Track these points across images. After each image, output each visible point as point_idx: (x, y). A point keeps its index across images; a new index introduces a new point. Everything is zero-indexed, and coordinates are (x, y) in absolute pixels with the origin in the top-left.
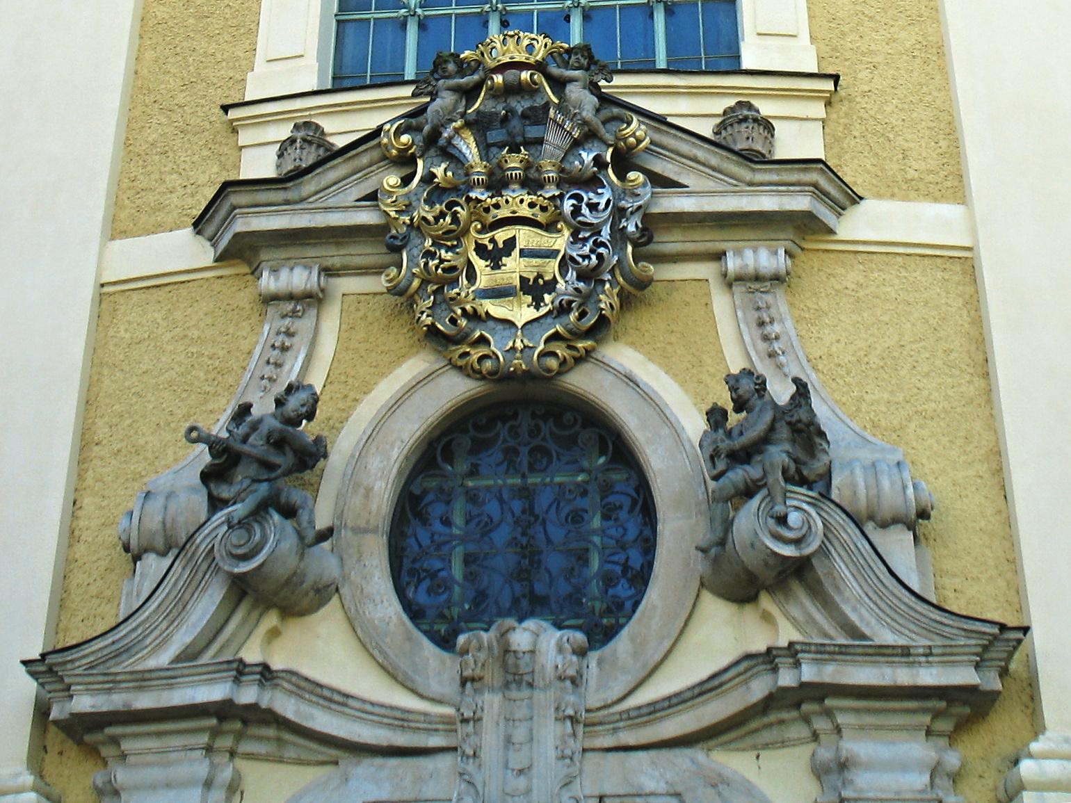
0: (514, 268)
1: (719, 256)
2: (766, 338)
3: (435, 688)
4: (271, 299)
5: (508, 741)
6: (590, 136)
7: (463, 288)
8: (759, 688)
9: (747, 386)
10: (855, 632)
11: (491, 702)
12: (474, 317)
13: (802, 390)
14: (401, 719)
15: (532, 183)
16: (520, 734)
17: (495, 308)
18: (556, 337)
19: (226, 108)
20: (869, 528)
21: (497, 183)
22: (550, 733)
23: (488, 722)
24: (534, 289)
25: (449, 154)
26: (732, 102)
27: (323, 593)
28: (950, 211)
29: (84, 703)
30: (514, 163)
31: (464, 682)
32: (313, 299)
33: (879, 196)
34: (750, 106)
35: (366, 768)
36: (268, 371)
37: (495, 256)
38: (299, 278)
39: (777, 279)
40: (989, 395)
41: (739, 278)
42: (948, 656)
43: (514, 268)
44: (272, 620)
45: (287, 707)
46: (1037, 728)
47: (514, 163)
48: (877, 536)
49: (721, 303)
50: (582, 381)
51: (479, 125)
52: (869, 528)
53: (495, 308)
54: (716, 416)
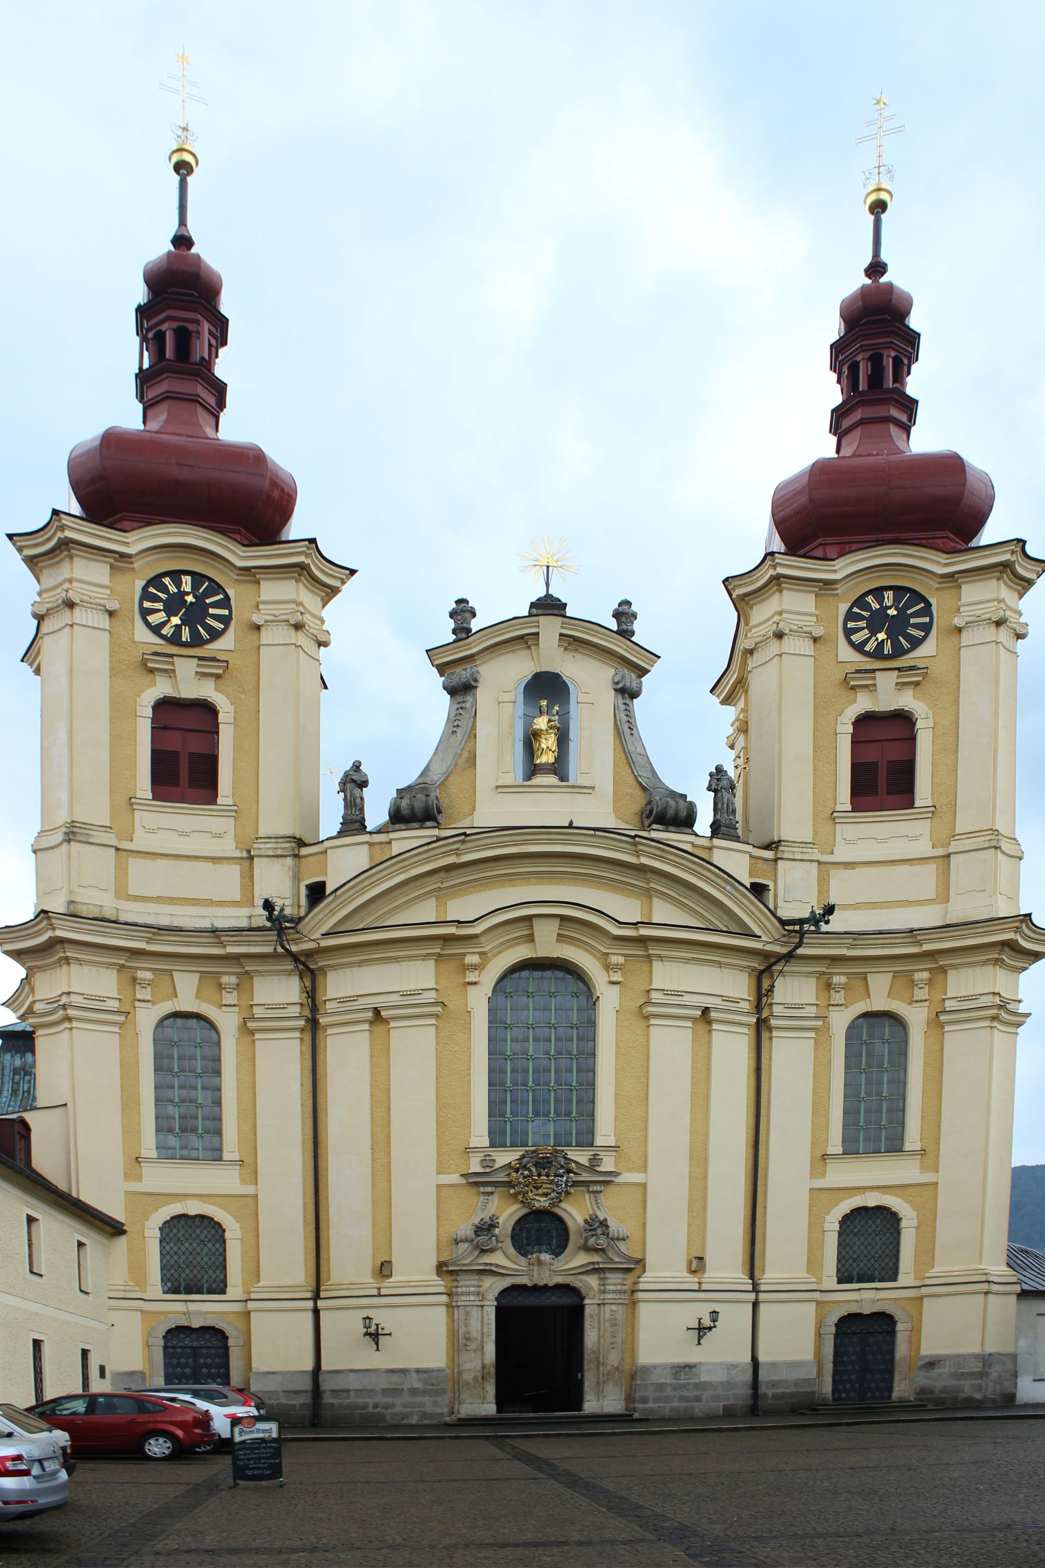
1: (588, 1186)
2: (597, 1204)
3: (523, 1264)
4: (483, 1193)
5: (539, 1274)
7: (530, 1195)
9: (594, 1217)
10: (611, 1259)
11: (536, 1268)
12: (532, 1199)
13: (605, 1220)
14: (517, 1270)
16: (542, 1273)
17: (537, 1198)
18: (550, 1203)
19: (466, 1149)
20: (615, 1241)
23: (535, 1271)
24: (546, 1195)
26: (593, 1153)
27: (498, 1249)
28: (643, 1175)
29: (451, 1268)
31: (530, 1264)
32: (492, 1193)
33: (626, 1172)
34: (598, 1155)
35: (509, 1278)
36: (484, 1207)
38: (490, 1189)
39: (600, 1192)
40: (645, 1212)
41: (592, 1192)
42: (630, 1263)
44: (488, 1253)
45: (494, 1269)
46: (644, 1271)
48: (617, 1243)
50: (556, 1210)
52: (615, 1241)
53: (537, 1198)
54: (586, 1221)
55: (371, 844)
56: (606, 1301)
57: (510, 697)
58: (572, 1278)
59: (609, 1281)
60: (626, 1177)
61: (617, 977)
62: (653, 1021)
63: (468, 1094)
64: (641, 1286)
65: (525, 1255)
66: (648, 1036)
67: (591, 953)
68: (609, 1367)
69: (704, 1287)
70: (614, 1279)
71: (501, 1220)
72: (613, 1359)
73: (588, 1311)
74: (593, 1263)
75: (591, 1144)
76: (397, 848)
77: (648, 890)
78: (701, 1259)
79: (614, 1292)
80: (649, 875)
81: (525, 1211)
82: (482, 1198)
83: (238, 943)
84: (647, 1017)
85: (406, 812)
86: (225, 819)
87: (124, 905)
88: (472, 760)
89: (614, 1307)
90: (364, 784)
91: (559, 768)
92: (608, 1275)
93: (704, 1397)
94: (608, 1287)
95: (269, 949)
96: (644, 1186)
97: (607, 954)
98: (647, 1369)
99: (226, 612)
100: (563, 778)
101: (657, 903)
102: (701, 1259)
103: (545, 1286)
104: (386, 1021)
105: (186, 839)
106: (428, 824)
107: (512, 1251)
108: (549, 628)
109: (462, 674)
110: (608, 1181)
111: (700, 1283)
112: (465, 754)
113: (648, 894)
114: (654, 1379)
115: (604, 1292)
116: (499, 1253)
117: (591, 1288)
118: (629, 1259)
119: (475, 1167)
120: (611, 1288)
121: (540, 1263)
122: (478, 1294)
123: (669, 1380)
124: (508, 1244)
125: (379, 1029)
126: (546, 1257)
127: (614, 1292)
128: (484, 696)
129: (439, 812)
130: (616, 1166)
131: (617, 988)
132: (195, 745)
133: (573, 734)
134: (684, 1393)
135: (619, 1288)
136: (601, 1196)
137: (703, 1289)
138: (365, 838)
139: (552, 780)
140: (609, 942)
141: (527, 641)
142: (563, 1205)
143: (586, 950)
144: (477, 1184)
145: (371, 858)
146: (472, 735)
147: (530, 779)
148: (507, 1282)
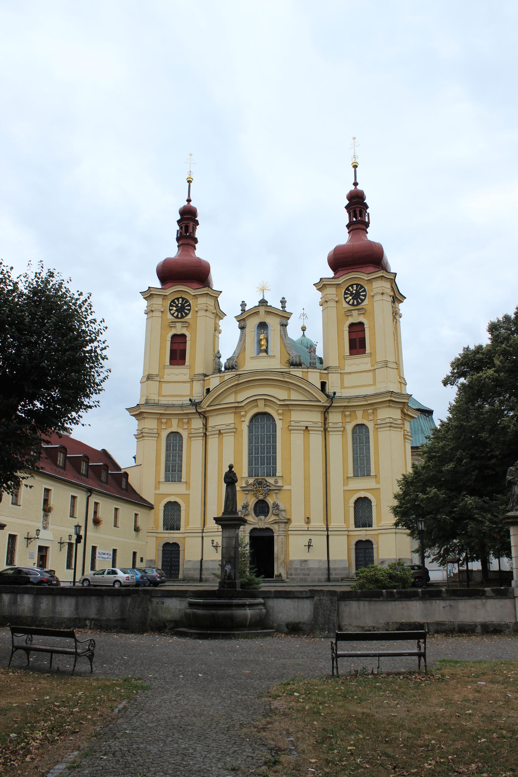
0: (260, 493)
6: (265, 484)
8: (275, 521)
14: (254, 522)
15: (261, 487)
21: (259, 487)
22: (263, 523)
25: (256, 485)
30: (260, 486)
37: (259, 492)
42: (285, 520)
43: (260, 493)
47: (260, 486)
49: (274, 495)
50: (265, 500)
51: (258, 484)
55: (220, 377)
56: (280, 534)
57: (253, 330)
58: (270, 525)
59: (281, 527)
60: (286, 487)
61: (281, 418)
62: (292, 432)
63: (242, 458)
64: (290, 529)
65: (257, 516)
66: (290, 437)
67: (274, 410)
68: (281, 561)
69: (310, 529)
70: (282, 525)
71: (250, 504)
72: (282, 557)
73: (275, 538)
74: (275, 520)
75: (276, 476)
76: (226, 378)
77: (290, 388)
78: (308, 518)
79: (282, 531)
80: (288, 383)
81: (257, 500)
82: (245, 495)
83: (187, 409)
84: (290, 430)
85: (228, 367)
86: (187, 369)
87: (161, 398)
88: (245, 349)
89: (282, 537)
90: (219, 358)
91: (266, 351)
92: (280, 524)
93: (311, 574)
94: (281, 529)
95: (195, 411)
96: (290, 490)
97: (278, 410)
98: (292, 562)
99: (189, 308)
100: (267, 354)
101: (292, 392)
102: (308, 518)
103: (263, 528)
104: (222, 434)
105: (177, 376)
106: (234, 370)
107: (254, 515)
108: (262, 310)
109: (242, 324)
110: (279, 489)
111: (308, 528)
112: (243, 348)
113: (289, 389)
114: (294, 566)
115: (279, 531)
116: (250, 516)
117: (276, 529)
118: (286, 519)
119: (244, 485)
120: (281, 529)
121: (261, 520)
122: (244, 531)
123: (299, 567)
124: (252, 512)
125: (221, 436)
126: (263, 517)
127: (282, 531)
128: (247, 329)
129: (236, 366)
130: (282, 483)
131: (281, 421)
132: (181, 347)
133: (269, 341)
134: (303, 572)
135: (283, 529)
136: (278, 494)
137: (309, 530)
138: (219, 375)
139: (264, 354)
140: (278, 406)
141: (257, 313)
142: (268, 498)
143: (273, 409)
144: (244, 491)
145: (220, 380)
146: (245, 341)
147: (258, 354)
148: (252, 527)
